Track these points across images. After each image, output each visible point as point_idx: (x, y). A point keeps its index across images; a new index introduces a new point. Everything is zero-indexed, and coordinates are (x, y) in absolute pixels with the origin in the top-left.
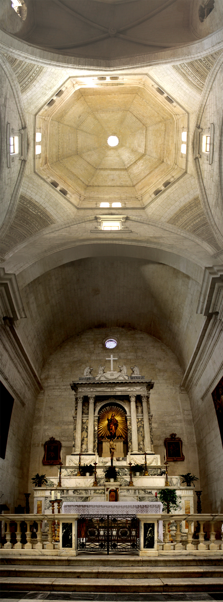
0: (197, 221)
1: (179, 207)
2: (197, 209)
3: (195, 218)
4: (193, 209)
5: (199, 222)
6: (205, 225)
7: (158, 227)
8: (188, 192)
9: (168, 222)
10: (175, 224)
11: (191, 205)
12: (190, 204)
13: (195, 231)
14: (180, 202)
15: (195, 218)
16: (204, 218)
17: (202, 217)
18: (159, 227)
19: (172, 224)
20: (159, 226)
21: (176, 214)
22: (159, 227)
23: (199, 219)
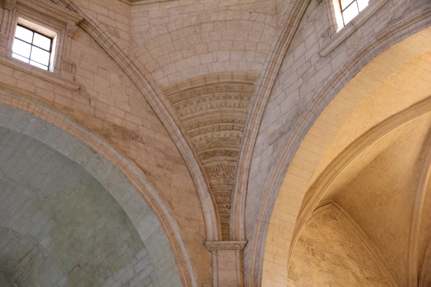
0: (222, 134)
1: (206, 70)
2: (237, 106)
3: (221, 124)
4: (230, 97)
5: (224, 139)
6: (230, 155)
7: (140, 90)
8: (245, 50)
9: (165, 91)
10: (178, 108)
11: (232, 85)
12: (230, 80)
13: (206, 155)
14: (215, 61)
15: (222, 122)
16: (238, 137)
17: (235, 133)
18: (142, 94)
19: (172, 103)
20: (144, 91)
21: (191, 81)
22: (142, 94)
23: (228, 133)
